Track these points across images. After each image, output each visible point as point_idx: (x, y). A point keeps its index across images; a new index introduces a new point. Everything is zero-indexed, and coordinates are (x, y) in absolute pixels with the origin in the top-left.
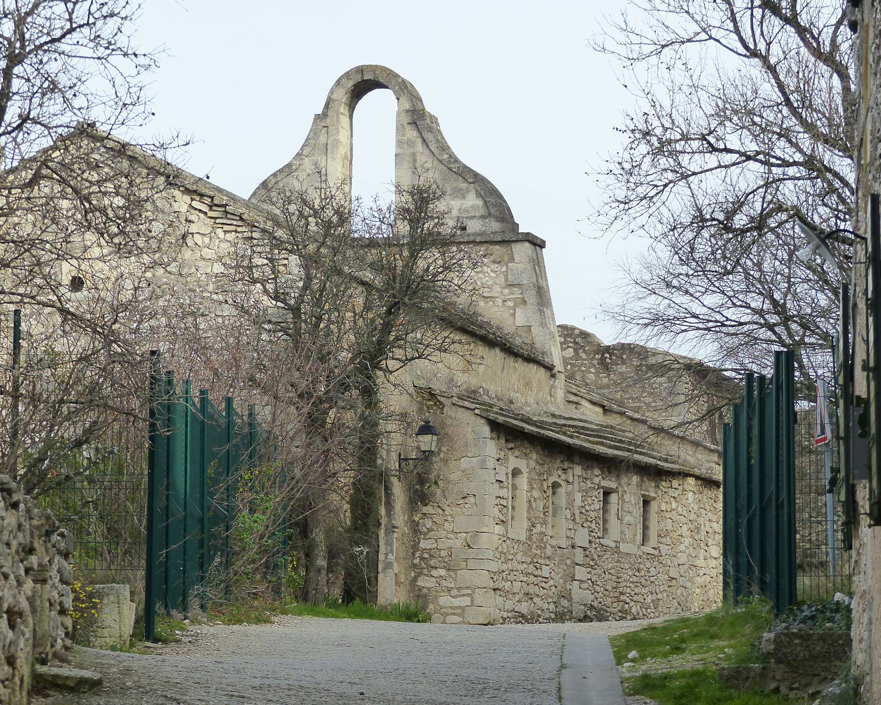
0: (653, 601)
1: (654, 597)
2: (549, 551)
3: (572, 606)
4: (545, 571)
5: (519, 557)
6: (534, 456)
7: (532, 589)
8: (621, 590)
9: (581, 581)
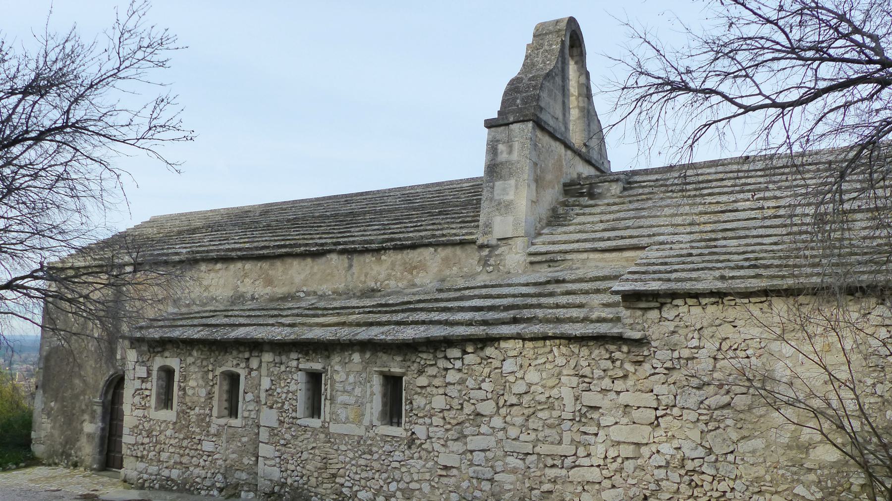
0: (398, 489)
1: (402, 485)
2: (213, 430)
3: (255, 478)
4: (208, 446)
5: (169, 433)
6: (195, 353)
7: (185, 460)
8: (334, 471)
9: (265, 458)
